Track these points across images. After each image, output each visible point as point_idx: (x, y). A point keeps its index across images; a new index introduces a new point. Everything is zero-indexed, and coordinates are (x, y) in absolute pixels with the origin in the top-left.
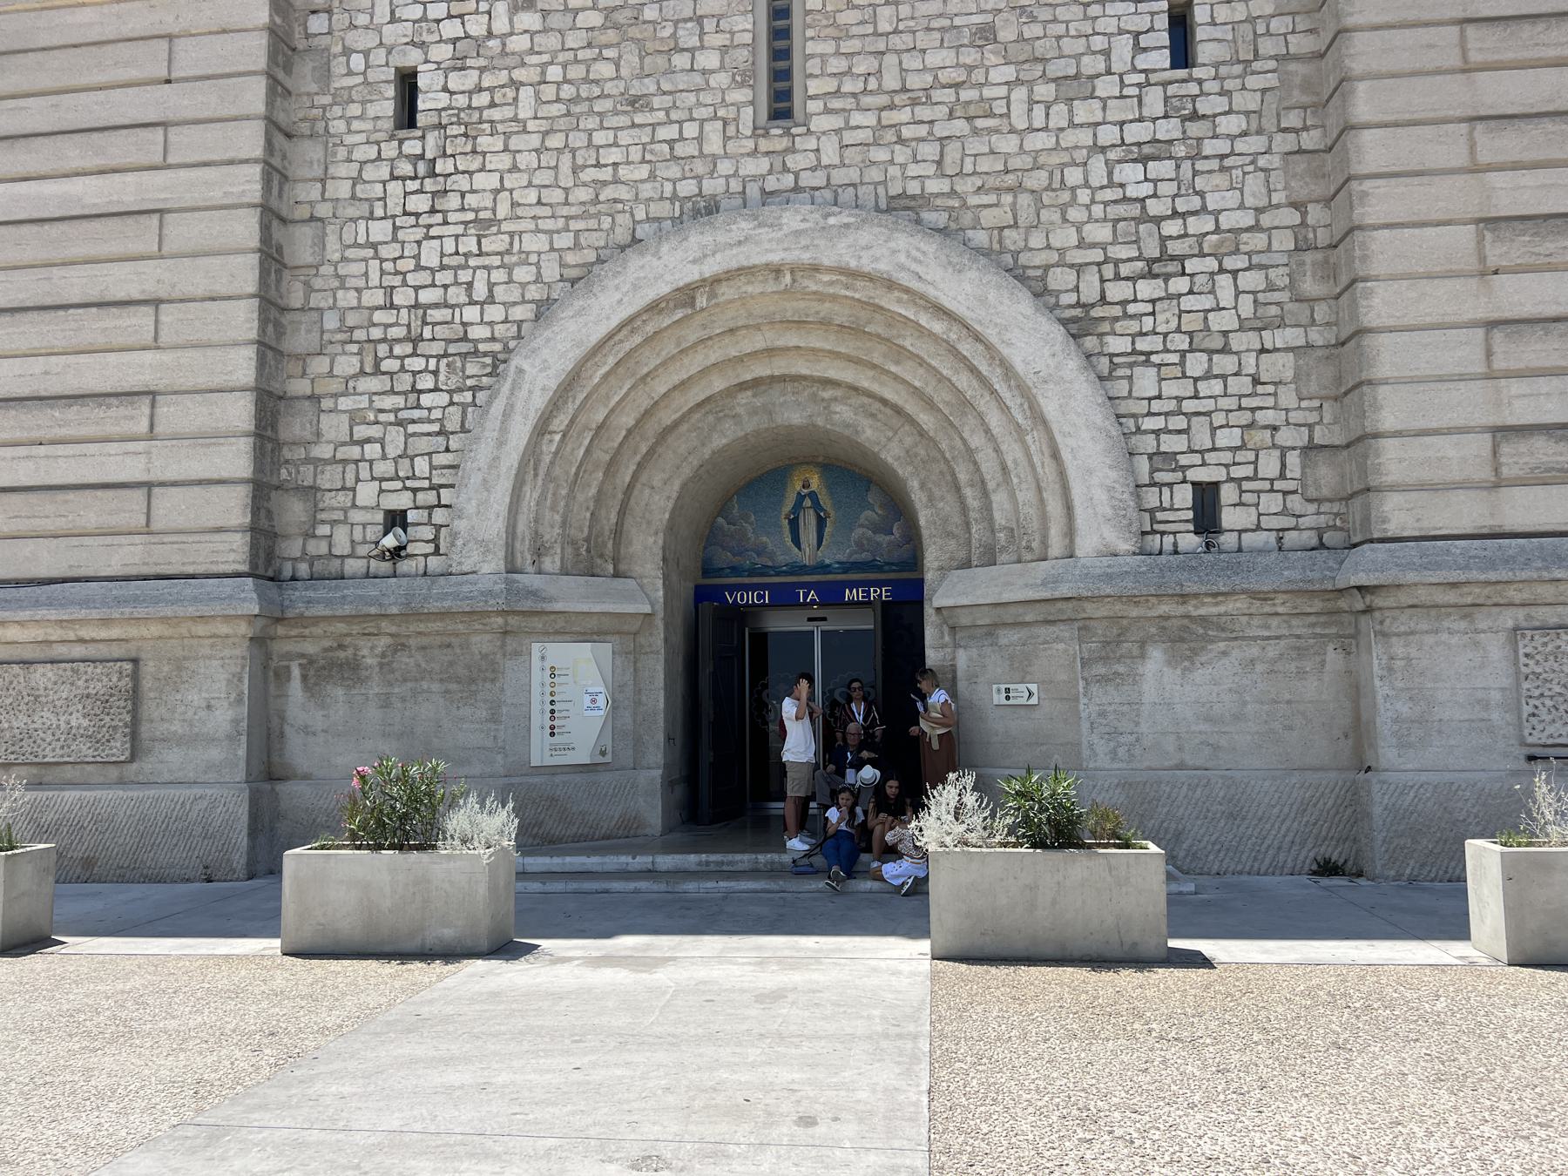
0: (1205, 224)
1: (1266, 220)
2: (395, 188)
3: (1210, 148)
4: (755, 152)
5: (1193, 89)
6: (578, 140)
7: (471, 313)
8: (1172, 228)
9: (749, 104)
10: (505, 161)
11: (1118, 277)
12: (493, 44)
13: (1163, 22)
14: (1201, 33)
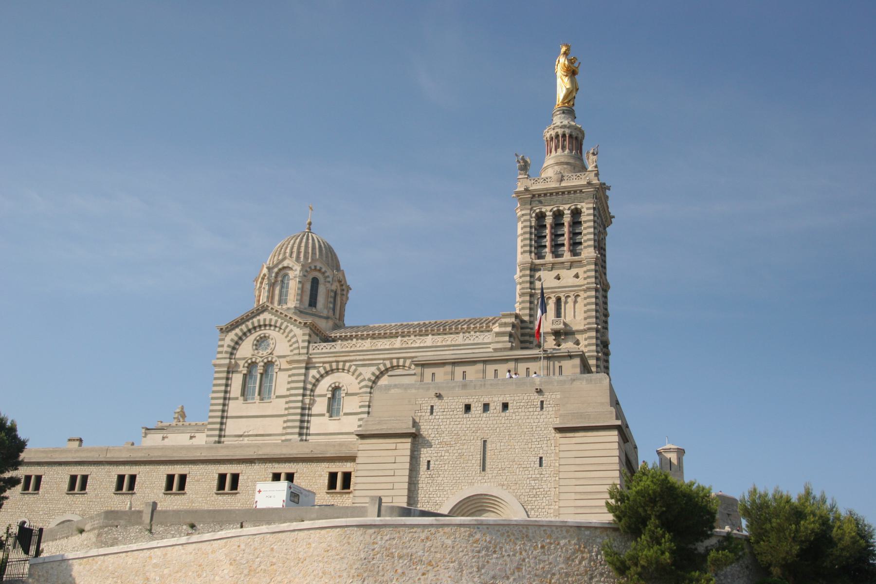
0: (542, 490)
1: (550, 490)
2: (426, 479)
3: (544, 479)
4: (480, 476)
5: (542, 470)
6: (454, 473)
7: (437, 499)
8: (538, 490)
9: (478, 468)
10: (443, 476)
11: (530, 497)
12: (442, 458)
13: (538, 460)
14: (543, 462)
